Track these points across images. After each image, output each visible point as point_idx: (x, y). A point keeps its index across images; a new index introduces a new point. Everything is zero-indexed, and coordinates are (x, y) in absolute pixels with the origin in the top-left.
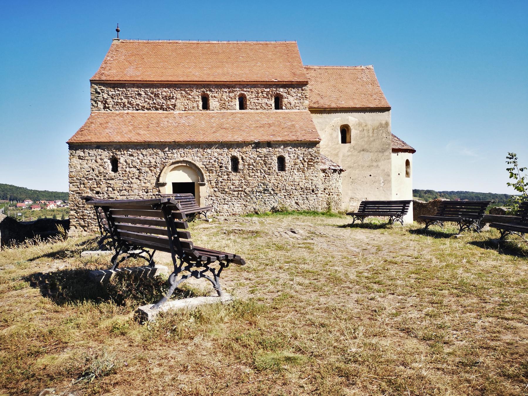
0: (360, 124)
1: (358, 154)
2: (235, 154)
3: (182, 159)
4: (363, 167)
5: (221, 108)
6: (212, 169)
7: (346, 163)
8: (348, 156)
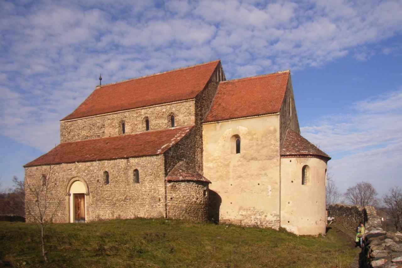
0: (249, 133)
1: (248, 163)
2: (107, 170)
3: (76, 175)
4: (252, 175)
5: (132, 131)
6: (93, 182)
7: (237, 172)
8: (239, 166)
